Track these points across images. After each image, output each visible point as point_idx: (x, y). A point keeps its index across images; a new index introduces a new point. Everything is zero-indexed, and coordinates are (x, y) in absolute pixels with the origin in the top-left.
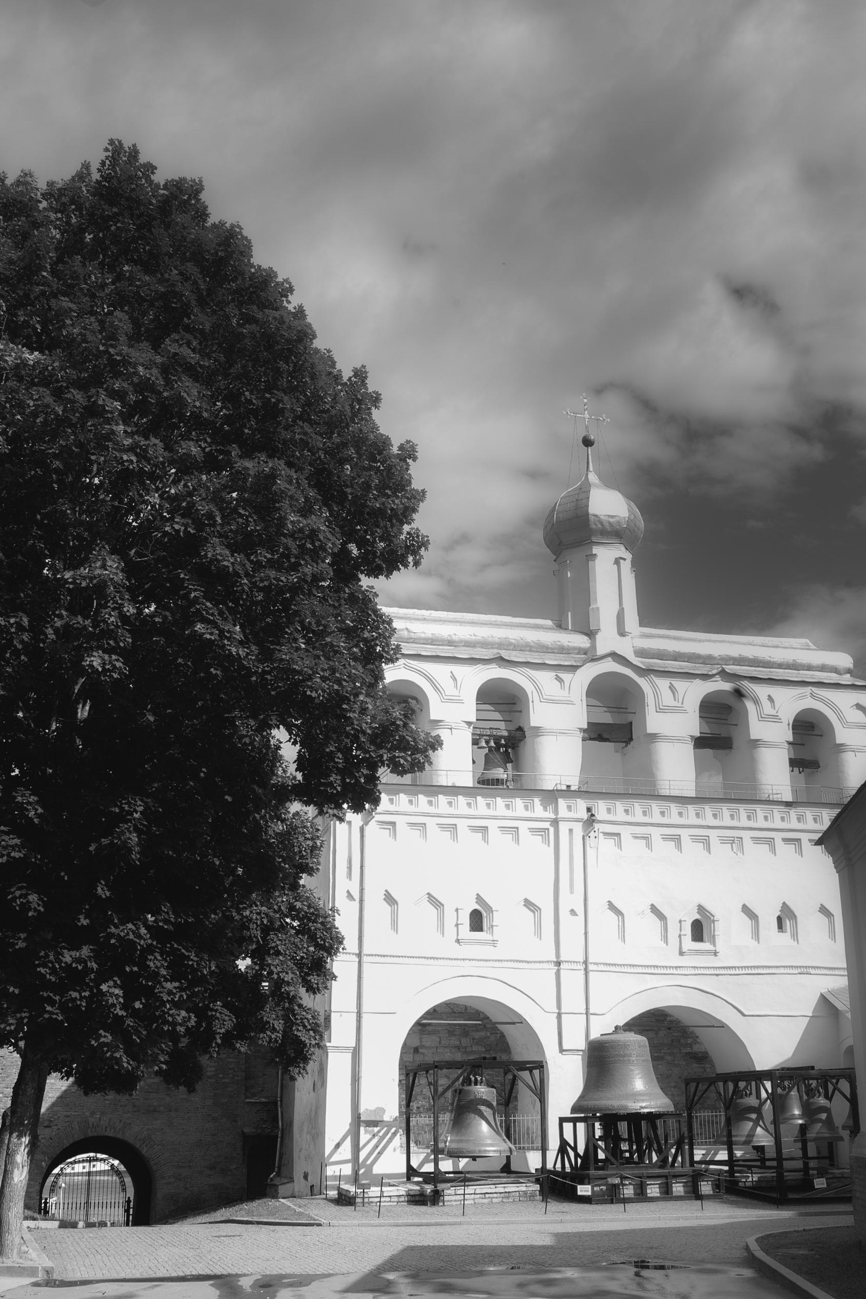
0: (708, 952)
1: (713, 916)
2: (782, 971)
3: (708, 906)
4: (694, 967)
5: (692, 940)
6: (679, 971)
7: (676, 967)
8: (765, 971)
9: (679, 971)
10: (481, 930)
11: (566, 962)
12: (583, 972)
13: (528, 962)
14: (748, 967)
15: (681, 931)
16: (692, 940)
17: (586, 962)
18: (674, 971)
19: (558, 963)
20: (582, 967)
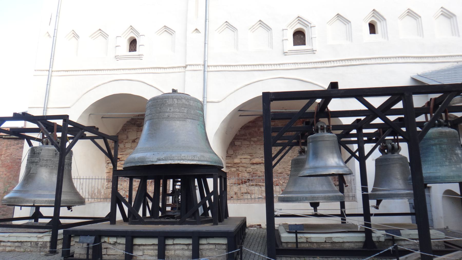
0: (306, 51)
1: (310, 24)
2: (373, 61)
3: (305, 16)
4: (295, 63)
5: (294, 45)
6: (282, 67)
7: (279, 64)
8: (358, 62)
9: (282, 67)
10: (135, 50)
11: (190, 65)
12: (203, 71)
13: (164, 68)
14: (342, 60)
15: (283, 36)
16: (294, 45)
17: (204, 65)
18: (278, 67)
19: (185, 67)
20: (201, 68)
